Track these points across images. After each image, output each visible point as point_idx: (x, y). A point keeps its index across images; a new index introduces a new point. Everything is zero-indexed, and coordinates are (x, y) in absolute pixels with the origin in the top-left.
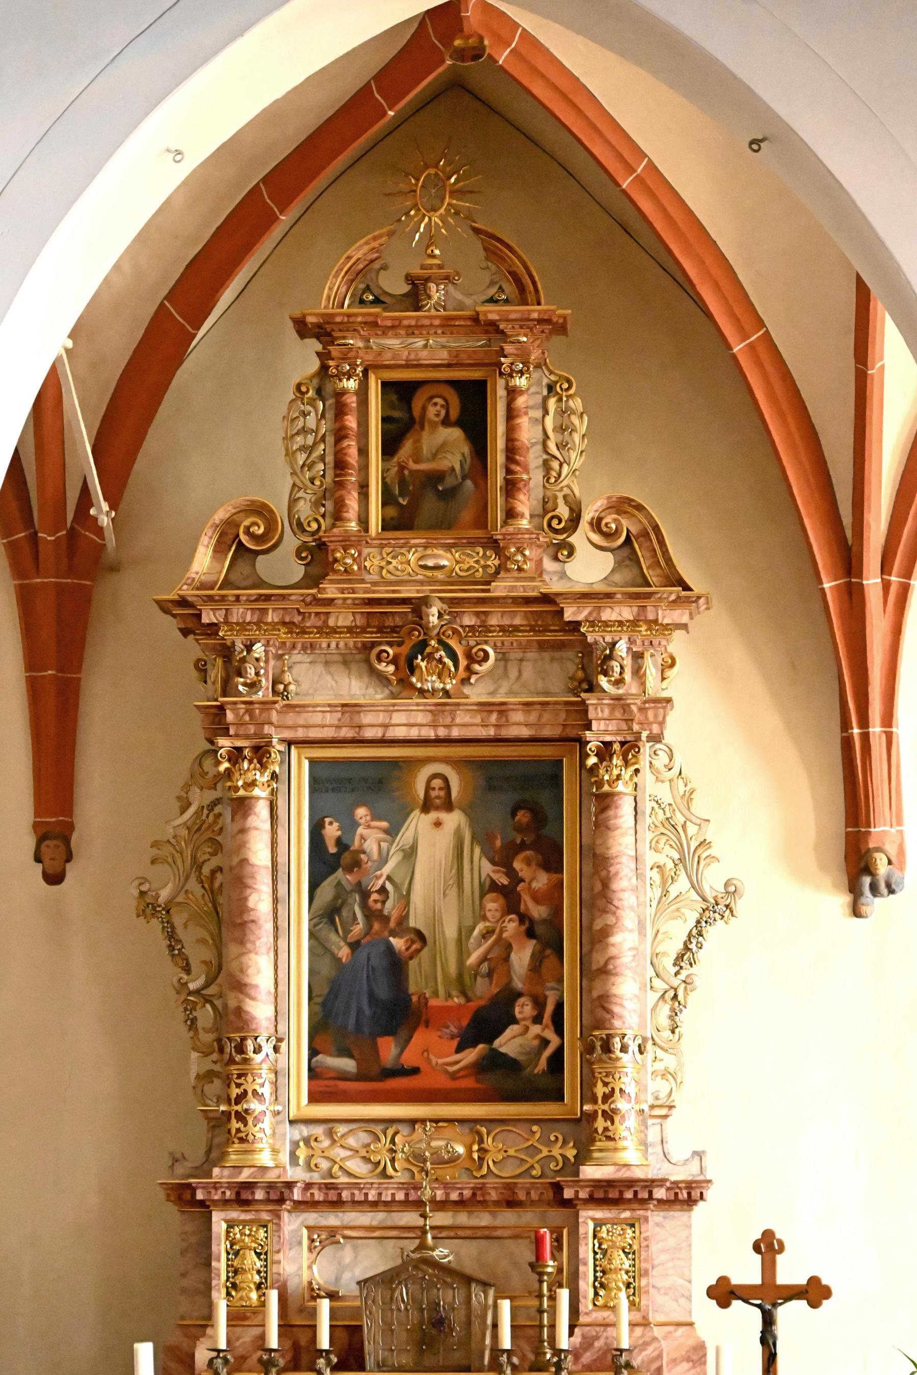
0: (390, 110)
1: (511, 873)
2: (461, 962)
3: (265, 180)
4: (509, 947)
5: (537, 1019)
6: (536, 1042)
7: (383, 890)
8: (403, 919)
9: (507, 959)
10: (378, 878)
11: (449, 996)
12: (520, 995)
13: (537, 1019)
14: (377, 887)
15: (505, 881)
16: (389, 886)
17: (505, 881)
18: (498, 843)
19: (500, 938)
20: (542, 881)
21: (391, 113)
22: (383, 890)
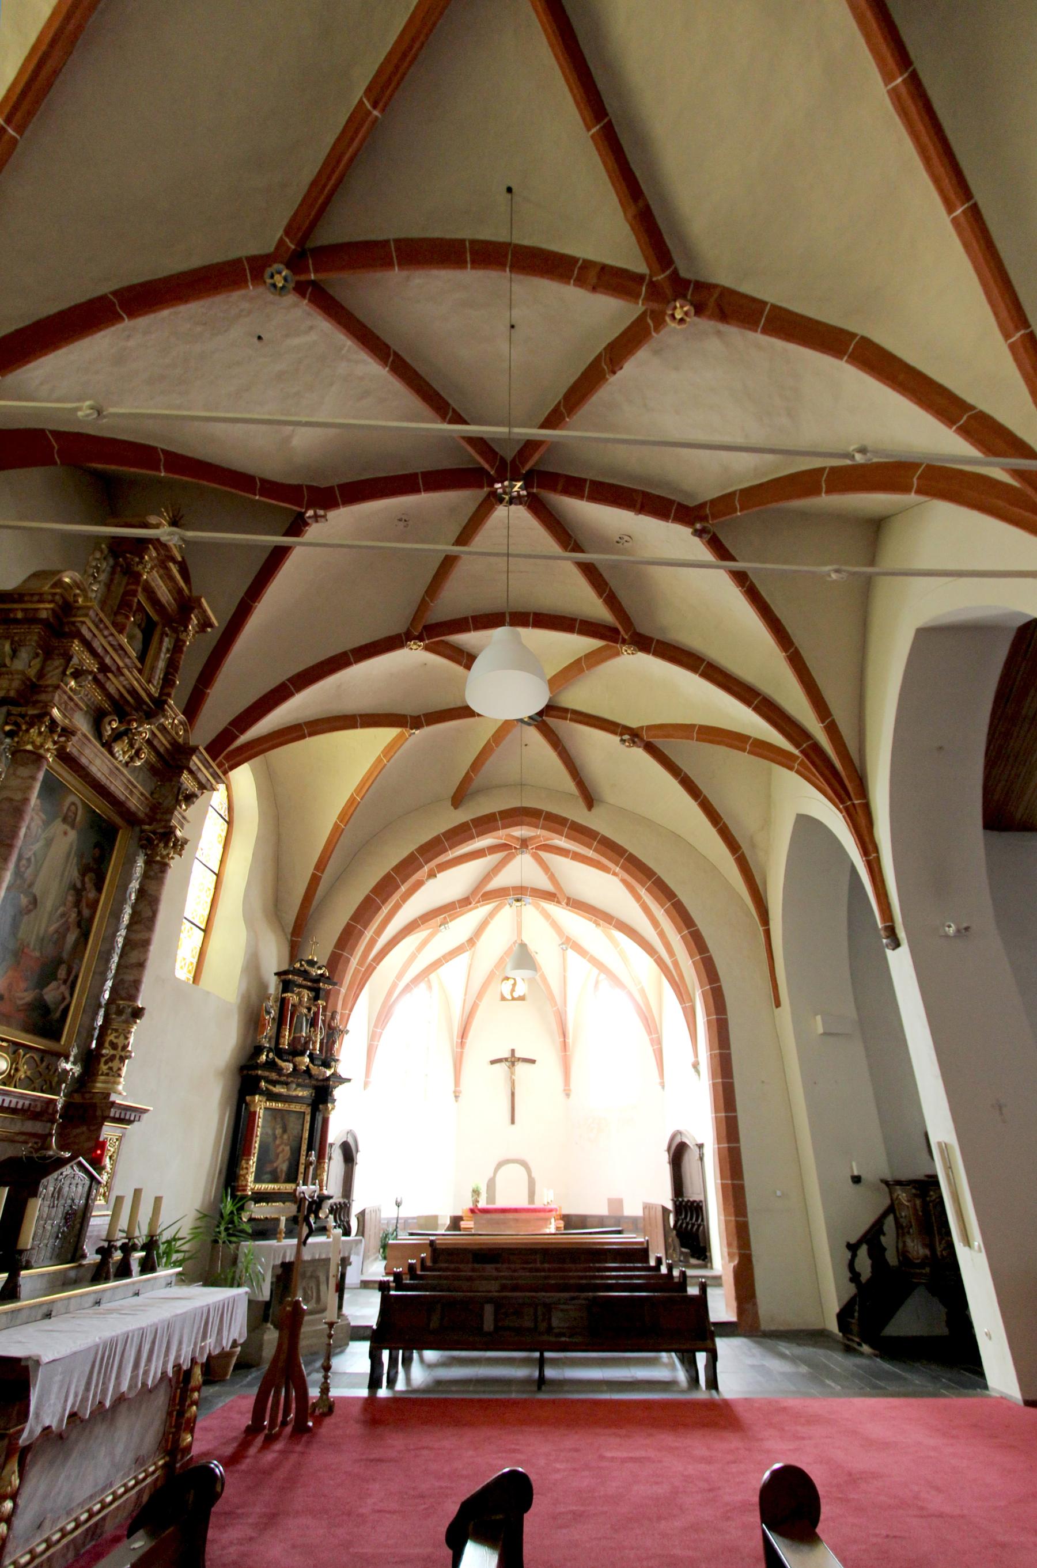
0: (740, 511)
1: (83, 882)
2: (46, 931)
3: (742, 491)
4: (68, 929)
5: (65, 982)
6: (60, 997)
7: (29, 860)
8: (31, 885)
9: (64, 937)
10: (30, 850)
11: (34, 949)
12: (64, 962)
13: (65, 982)
14: (28, 857)
15: (79, 885)
16: (33, 859)
17: (79, 885)
18: (84, 861)
19: (67, 921)
20: (92, 895)
21: (739, 514)
22: (29, 860)
